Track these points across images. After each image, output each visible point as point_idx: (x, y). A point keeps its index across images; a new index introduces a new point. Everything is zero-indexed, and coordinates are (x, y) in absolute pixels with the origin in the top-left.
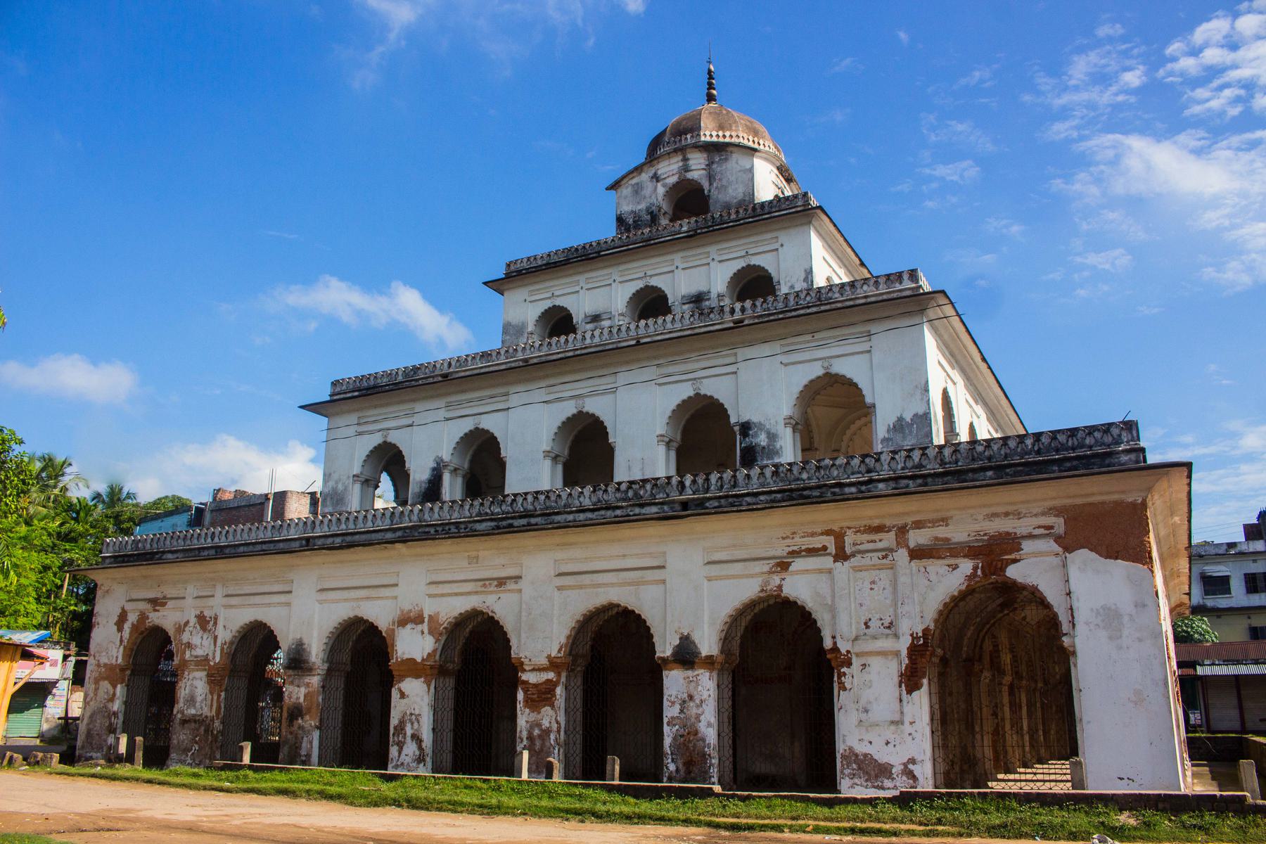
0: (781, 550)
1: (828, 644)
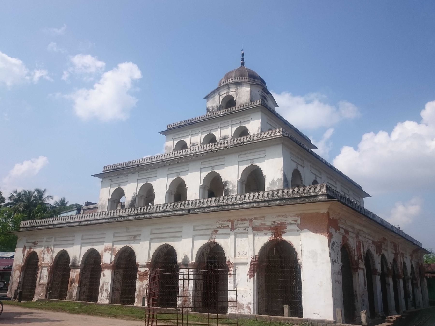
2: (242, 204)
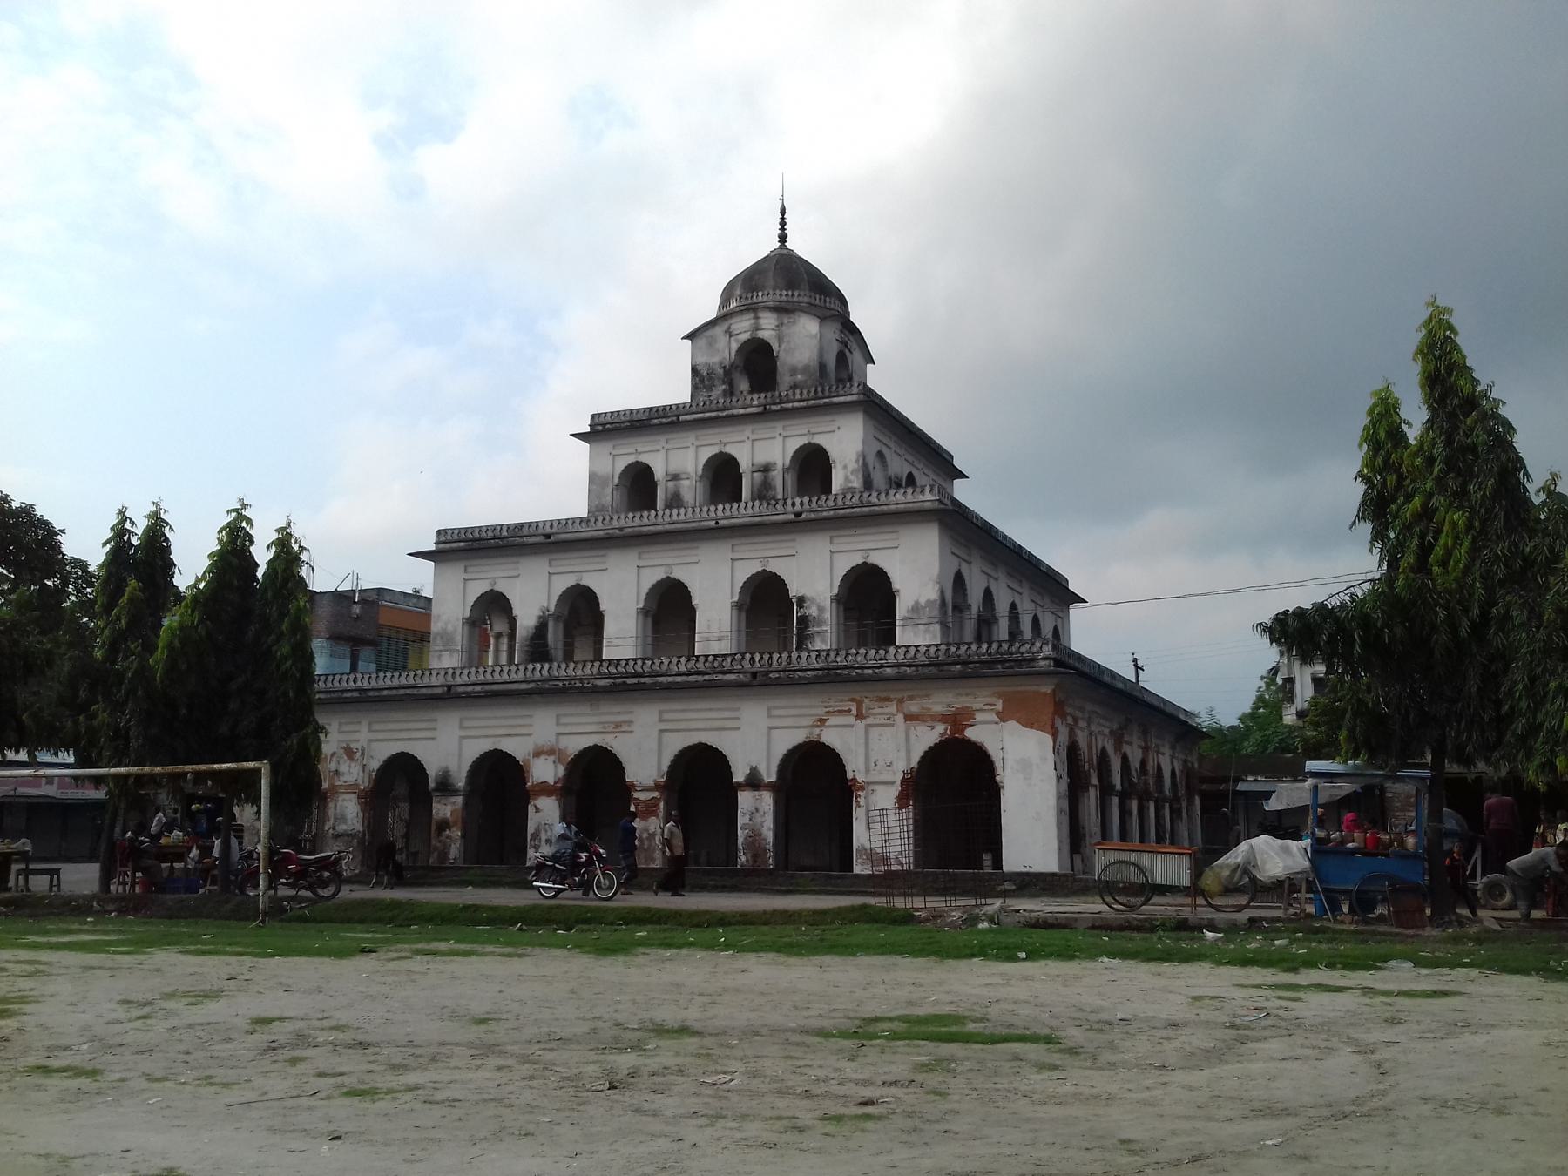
0: (821, 711)
1: (850, 776)
2: (882, 666)
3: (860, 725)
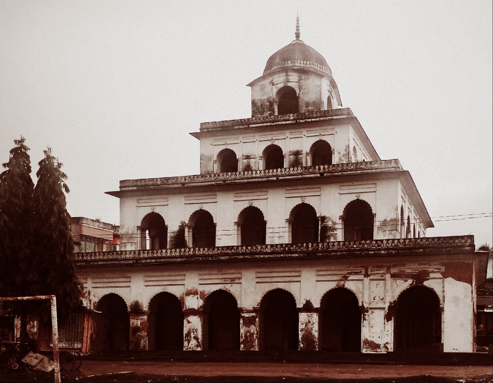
1: (360, 304)
3: (366, 280)
